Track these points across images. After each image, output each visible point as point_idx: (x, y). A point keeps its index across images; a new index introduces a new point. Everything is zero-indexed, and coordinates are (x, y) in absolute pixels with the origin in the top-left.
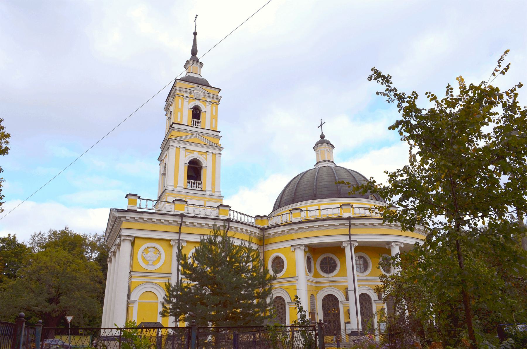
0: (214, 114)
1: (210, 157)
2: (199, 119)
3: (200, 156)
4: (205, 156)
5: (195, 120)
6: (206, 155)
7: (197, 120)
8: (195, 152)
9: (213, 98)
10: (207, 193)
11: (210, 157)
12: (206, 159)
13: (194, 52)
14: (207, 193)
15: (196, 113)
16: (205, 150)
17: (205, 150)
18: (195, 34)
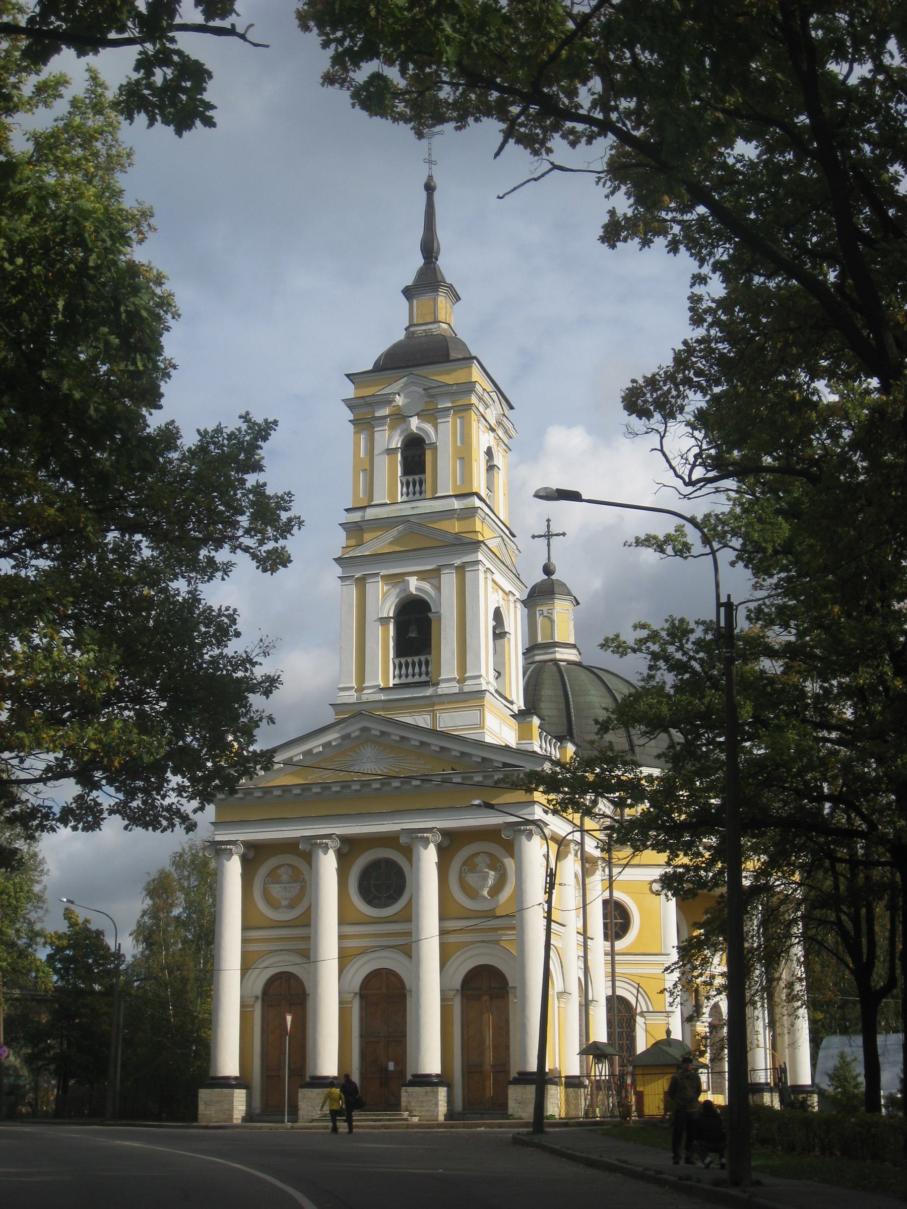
1: (449, 580)
4: (435, 581)
7: (417, 478)
10: (443, 688)
12: (438, 589)
13: (429, 249)
14: (443, 688)
15: (415, 457)
18: (430, 188)
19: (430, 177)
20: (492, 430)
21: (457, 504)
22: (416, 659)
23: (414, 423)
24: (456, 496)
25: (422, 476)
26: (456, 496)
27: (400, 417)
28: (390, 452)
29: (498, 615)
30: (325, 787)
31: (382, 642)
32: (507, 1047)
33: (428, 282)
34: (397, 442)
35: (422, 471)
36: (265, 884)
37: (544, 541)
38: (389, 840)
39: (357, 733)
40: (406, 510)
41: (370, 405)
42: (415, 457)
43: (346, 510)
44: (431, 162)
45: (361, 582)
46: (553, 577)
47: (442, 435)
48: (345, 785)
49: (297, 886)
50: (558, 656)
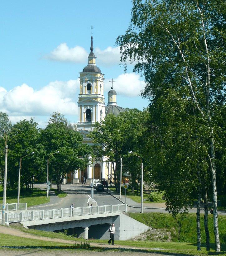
1: (94, 108)
13: (92, 50)
15: (89, 87)
18: (92, 38)
21: (95, 96)
23: (89, 82)
27: (86, 81)
28: (85, 86)
29: (101, 111)
31: (84, 116)
33: (91, 56)
34: (86, 85)
35: (90, 89)
37: (111, 83)
40: (88, 96)
42: (89, 87)
44: (92, 33)
46: (113, 89)
47: (93, 84)
50: (113, 105)
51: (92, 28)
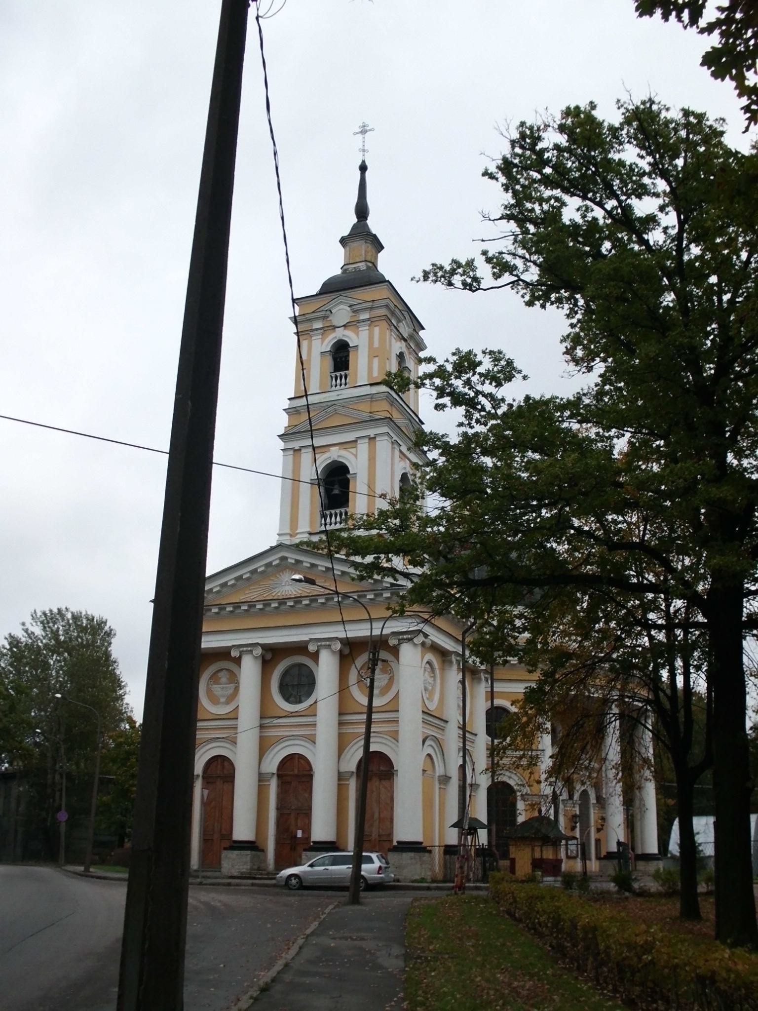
0: (376, 344)
1: (363, 447)
2: (347, 368)
3: (343, 453)
4: (353, 450)
5: (338, 374)
6: (356, 447)
7: (343, 373)
8: (333, 449)
9: (371, 308)
11: (363, 447)
12: (356, 456)
13: (362, 211)
15: (341, 356)
16: (350, 436)
17: (350, 436)
18: (363, 168)
19: (364, 162)
20: (405, 340)
22: (338, 511)
24: (371, 385)
25: (347, 372)
26: (371, 385)
30: (251, 605)
32: (391, 820)
36: (208, 685)
38: (300, 648)
39: (277, 562)
40: (332, 396)
41: (309, 320)
42: (341, 356)
43: (289, 399)
44: (364, 151)
45: (297, 451)
48: (267, 603)
49: (232, 686)
51: (364, 131)
